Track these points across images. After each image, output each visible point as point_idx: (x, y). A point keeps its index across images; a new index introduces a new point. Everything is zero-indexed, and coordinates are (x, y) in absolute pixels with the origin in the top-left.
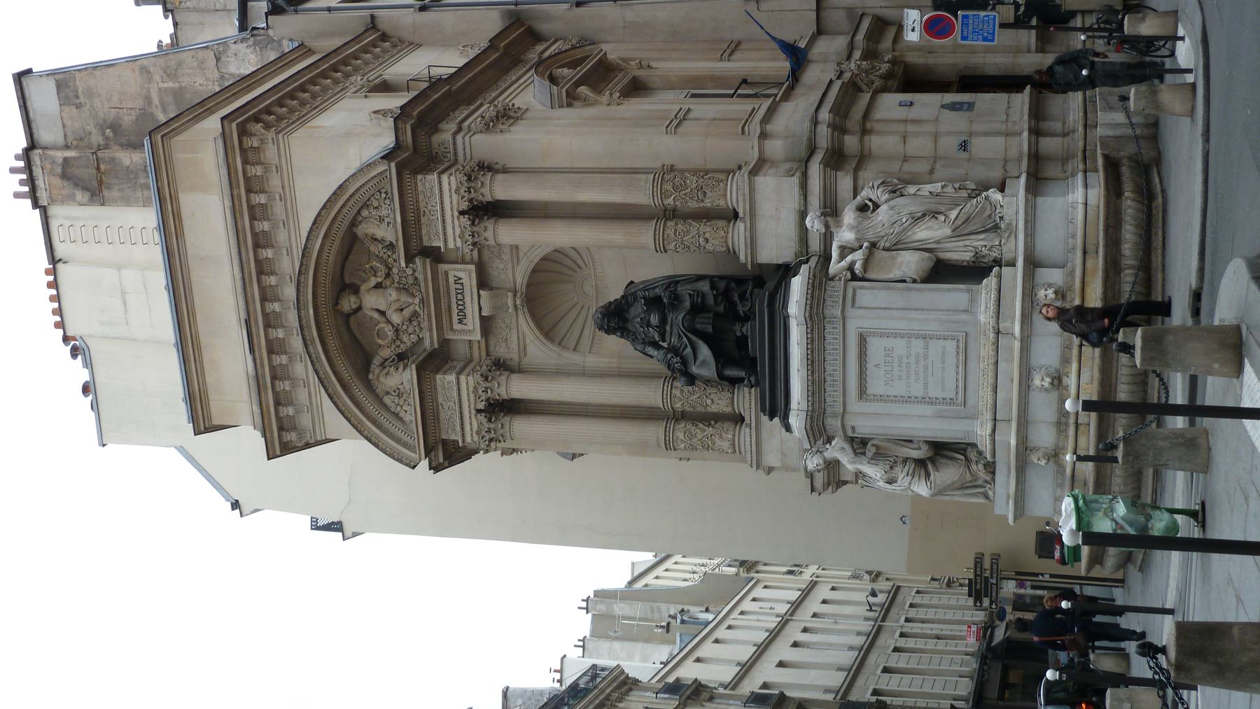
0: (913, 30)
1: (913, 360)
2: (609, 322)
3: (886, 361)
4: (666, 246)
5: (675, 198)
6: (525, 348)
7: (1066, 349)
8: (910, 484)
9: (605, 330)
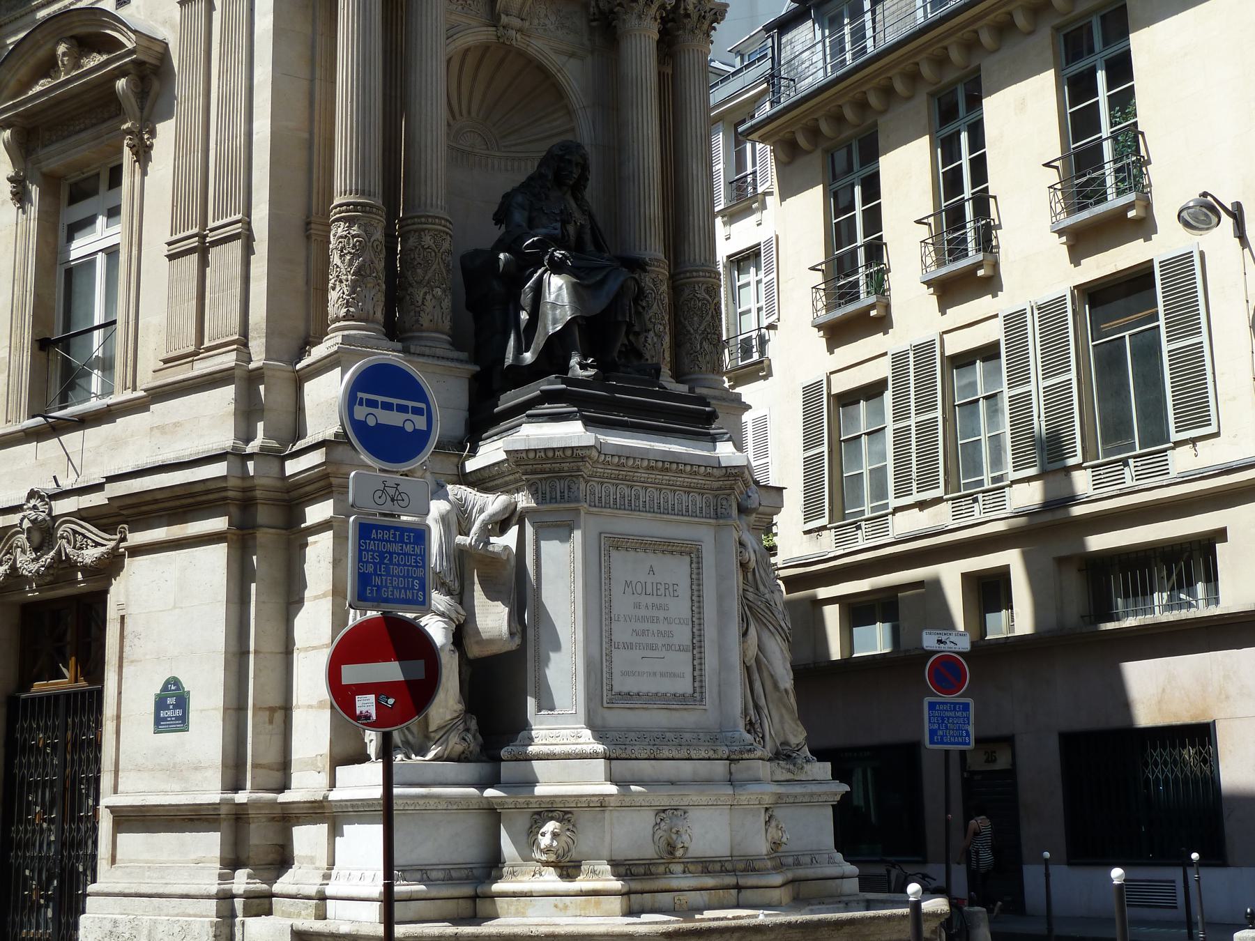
0: (940, 641)
1: (663, 627)
3: (659, 586)
5: (708, 301)
7: (719, 864)
8: (442, 615)
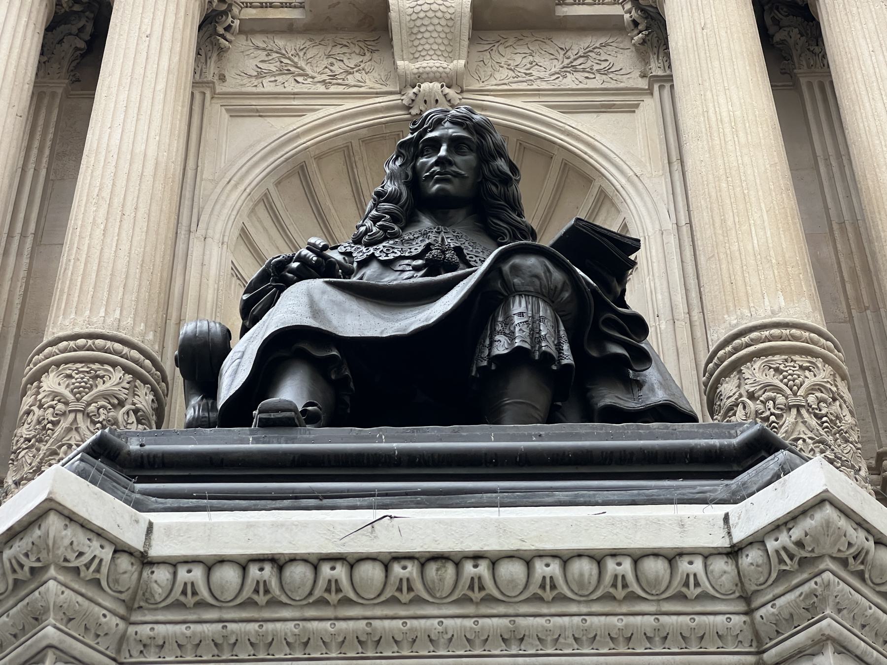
2: (455, 143)
4: (758, 363)
6: (259, 113)
9: (421, 136)
